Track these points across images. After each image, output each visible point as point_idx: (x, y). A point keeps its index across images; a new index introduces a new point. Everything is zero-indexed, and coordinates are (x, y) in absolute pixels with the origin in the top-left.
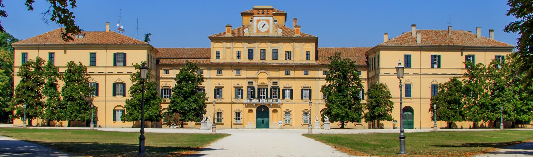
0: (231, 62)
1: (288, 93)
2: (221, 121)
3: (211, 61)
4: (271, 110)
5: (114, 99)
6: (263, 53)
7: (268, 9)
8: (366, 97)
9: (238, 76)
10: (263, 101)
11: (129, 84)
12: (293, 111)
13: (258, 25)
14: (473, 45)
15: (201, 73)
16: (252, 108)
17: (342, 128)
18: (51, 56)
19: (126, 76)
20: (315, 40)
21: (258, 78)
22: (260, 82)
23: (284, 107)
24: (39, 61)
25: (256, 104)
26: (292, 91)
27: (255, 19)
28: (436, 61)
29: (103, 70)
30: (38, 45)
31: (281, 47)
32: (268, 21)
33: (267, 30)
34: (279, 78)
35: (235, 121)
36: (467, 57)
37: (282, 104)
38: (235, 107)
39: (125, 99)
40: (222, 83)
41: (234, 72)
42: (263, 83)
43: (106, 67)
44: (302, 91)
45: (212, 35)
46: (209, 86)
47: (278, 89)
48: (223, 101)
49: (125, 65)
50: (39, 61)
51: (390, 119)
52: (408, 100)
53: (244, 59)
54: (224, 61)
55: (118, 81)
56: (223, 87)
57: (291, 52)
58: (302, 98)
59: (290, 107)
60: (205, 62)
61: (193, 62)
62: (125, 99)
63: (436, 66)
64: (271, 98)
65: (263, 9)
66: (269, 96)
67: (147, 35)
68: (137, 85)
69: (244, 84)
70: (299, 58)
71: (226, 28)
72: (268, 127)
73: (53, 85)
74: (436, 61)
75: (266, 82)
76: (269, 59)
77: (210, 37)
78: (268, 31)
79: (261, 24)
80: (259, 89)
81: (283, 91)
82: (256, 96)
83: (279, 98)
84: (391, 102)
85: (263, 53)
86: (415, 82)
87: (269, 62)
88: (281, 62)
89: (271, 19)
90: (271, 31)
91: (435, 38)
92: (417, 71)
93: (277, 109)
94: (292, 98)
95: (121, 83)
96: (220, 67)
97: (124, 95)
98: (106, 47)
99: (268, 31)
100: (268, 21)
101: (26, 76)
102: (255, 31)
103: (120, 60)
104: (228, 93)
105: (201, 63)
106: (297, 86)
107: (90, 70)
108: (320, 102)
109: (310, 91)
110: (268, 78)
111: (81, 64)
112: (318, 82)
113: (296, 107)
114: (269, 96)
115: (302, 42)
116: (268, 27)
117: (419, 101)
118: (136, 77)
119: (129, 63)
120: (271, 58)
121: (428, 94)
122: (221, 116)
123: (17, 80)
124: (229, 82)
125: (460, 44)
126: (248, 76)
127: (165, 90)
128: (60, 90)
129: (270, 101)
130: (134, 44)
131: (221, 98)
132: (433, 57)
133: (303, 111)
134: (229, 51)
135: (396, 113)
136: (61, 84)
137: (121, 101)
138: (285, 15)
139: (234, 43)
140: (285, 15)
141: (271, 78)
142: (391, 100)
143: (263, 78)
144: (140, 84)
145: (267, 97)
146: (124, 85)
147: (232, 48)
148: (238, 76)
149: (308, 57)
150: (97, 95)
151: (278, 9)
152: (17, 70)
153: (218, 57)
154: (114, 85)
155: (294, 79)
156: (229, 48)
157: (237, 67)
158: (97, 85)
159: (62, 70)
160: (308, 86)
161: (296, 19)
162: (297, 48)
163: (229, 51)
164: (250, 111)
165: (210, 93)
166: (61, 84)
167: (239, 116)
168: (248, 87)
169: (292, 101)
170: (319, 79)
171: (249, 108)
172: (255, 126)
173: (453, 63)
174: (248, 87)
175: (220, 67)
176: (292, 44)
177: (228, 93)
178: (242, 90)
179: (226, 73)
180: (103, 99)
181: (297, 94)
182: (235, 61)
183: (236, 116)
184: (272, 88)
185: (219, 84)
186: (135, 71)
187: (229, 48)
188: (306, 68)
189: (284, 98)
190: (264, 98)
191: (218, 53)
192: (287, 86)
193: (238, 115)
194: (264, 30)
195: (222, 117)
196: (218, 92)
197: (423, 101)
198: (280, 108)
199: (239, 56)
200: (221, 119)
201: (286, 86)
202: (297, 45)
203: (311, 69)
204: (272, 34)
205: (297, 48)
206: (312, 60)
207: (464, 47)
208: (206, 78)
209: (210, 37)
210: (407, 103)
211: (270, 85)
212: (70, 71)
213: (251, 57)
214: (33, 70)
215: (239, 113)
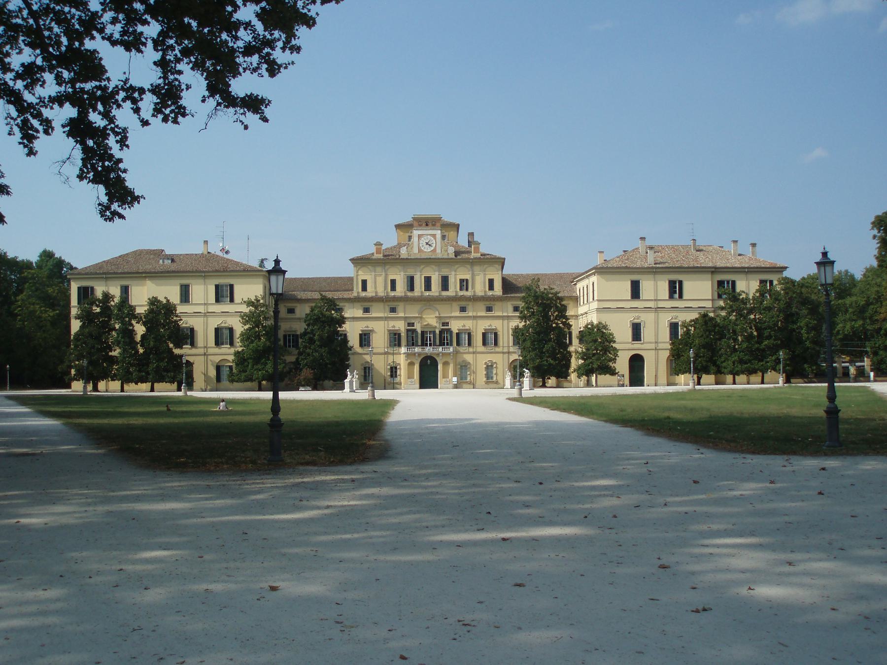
3: (355, 294)
5: (217, 350)
6: (428, 280)
8: (575, 341)
9: (393, 315)
10: (428, 350)
11: (239, 328)
14: (728, 265)
15: (340, 310)
16: (414, 361)
17: (544, 386)
18: (125, 290)
19: (233, 316)
20: (502, 262)
21: (421, 318)
24: (107, 297)
25: (419, 354)
26: (469, 335)
27: (416, 233)
28: (675, 290)
29: (201, 309)
30: (105, 273)
32: (434, 236)
36: (720, 283)
38: (391, 357)
39: (232, 350)
40: (371, 325)
41: (388, 309)
43: (205, 304)
44: (484, 335)
46: (352, 330)
47: (449, 331)
48: (375, 351)
49: (232, 300)
50: (107, 297)
51: (613, 372)
52: (637, 345)
55: (223, 325)
56: (372, 331)
57: (467, 280)
60: (346, 295)
61: (329, 295)
62: (232, 350)
63: (677, 296)
64: (442, 344)
66: (438, 342)
67: (262, 261)
68: (250, 329)
69: (401, 326)
70: (479, 287)
72: (436, 386)
73: (128, 333)
74: (675, 290)
77: (353, 260)
78: (434, 250)
79: (423, 241)
80: (423, 332)
82: (420, 343)
83: (451, 345)
84: (615, 349)
85: (428, 280)
86: (648, 320)
87: (437, 294)
89: (438, 233)
90: (438, 250)
91: (673, 255)
92: (651, 304)
94: (469, 344)
95: (226, 328)
96: (367, 304)
97: (232, 344)
98: (202, 274)
100: (434, 236)
101: (87, 317)
102: (416, 250)
103: (224, 294)
104: (380, 341)
105: (341, 297)
107: (180, 309)
108: (511, 349)
109: (496, 334)
111: (168, 301)
112: (507, 322)
113: (478, 358)
117: (653, 346)
118: (246, 318)
119: (237, 298)
121: (665, 335)
123: (76, 326)
125: (710, 265)
127: (289, 335)
128: (138, 338)
129: (440, 349)
130: (244, 271)
131: (369, 345)
132: (672, 284)
134: (380, 280)
135: (622, 365)
136: (140, 330)
137: (227, 354)
138: (456, 227)
140: (456, 227)
142: (614, 345)
144: (253, 328)
146: (231, 330)
147: (386, 275)
149: (491, 287)
150: (193, 344)
151: (447, 218)
152: (74, 311)
153: (364, 288)
154: (217, 330)
155: (475, 318)
158: (192, 330)
159: (141, 310)
161: (471, 235)
165: (354, 341)
166: (140, 330)
167: (396, 372)
168: (408, 330)
169: (471, 350)
172: (418, 385)
173: (700, 293)
174: (408, 330)
175: (367, 304)
178: (399, 335)
180: (201, 351)
181: (478, 339)
184: (441, 332)
186: (245, 309)
188: (489, 303)
189: (458, 344)
190: (430, 345)
191: (364, 282)
193: (394, 371)
196: (365, 339)
197: (661, 346)
202: (477, 268)
204: (439, 254)
206: (498, 290)
207: (716, 268)
209: (353, 260)
210: (637, 348)
212: (151, 311)
213: (411, 286)
214: (98, 310)
215: (396, 368)
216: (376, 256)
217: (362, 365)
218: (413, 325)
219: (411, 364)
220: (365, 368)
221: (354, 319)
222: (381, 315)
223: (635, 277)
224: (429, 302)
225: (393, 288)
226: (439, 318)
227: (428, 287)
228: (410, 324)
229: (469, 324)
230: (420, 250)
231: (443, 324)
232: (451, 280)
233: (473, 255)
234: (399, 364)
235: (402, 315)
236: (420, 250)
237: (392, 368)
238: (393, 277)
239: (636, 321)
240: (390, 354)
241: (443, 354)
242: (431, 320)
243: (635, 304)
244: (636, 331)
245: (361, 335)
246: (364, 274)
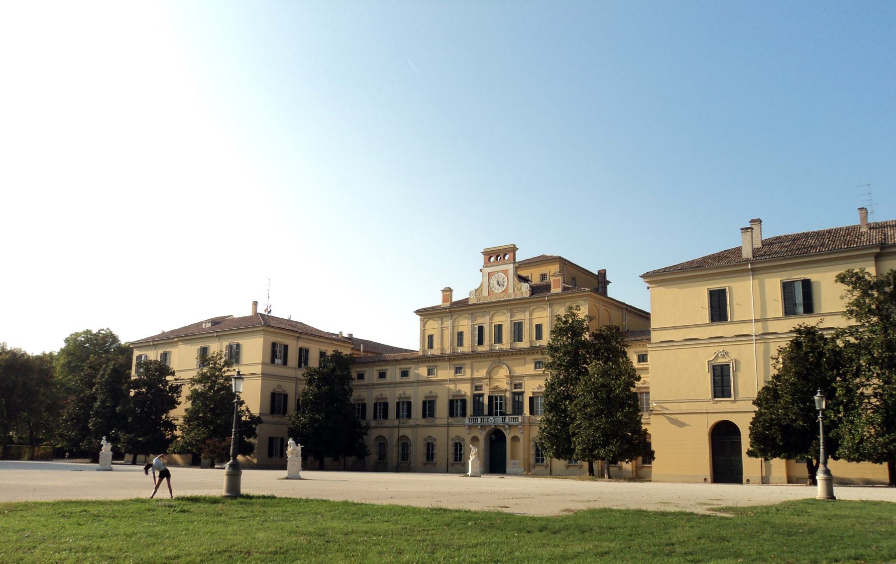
35: (451, 460)
42: (497, 387)
48: (438, 422)
52: (724, 404)
56: (436, 397)
63: (801, 309)
77: (418, 312)
78: (506, 291)
81: (531, 399)
100: (506, 272)
116: (506, 284)
122: (433, 450)
126: (476, 375)
157: (456, 360)
168: (475, 396)
174: (475, 396)
177: (442, 409)
178: (464, 402)
183: (456, 450)
189: (532, 412)
194: (498, 290)
200: (433, 454)
201: (536, 390)
209: (418, 312)
217: (425, 439)
220: (429, 444)
223: (717, 285)
224: (497, 357)
225: (460, 343)
226: (511, 377)
227: (499, 339)
228: (477, 388)
232: (526, 328)
234: (463, 440)
235: (468, 375)
239: (721, 361)
240: (453, 425)
241: (510, 426)
242: (501, 380)
243: (720, 329)
244: (722, 381)
245: (424, 403)
246: (433, 326)
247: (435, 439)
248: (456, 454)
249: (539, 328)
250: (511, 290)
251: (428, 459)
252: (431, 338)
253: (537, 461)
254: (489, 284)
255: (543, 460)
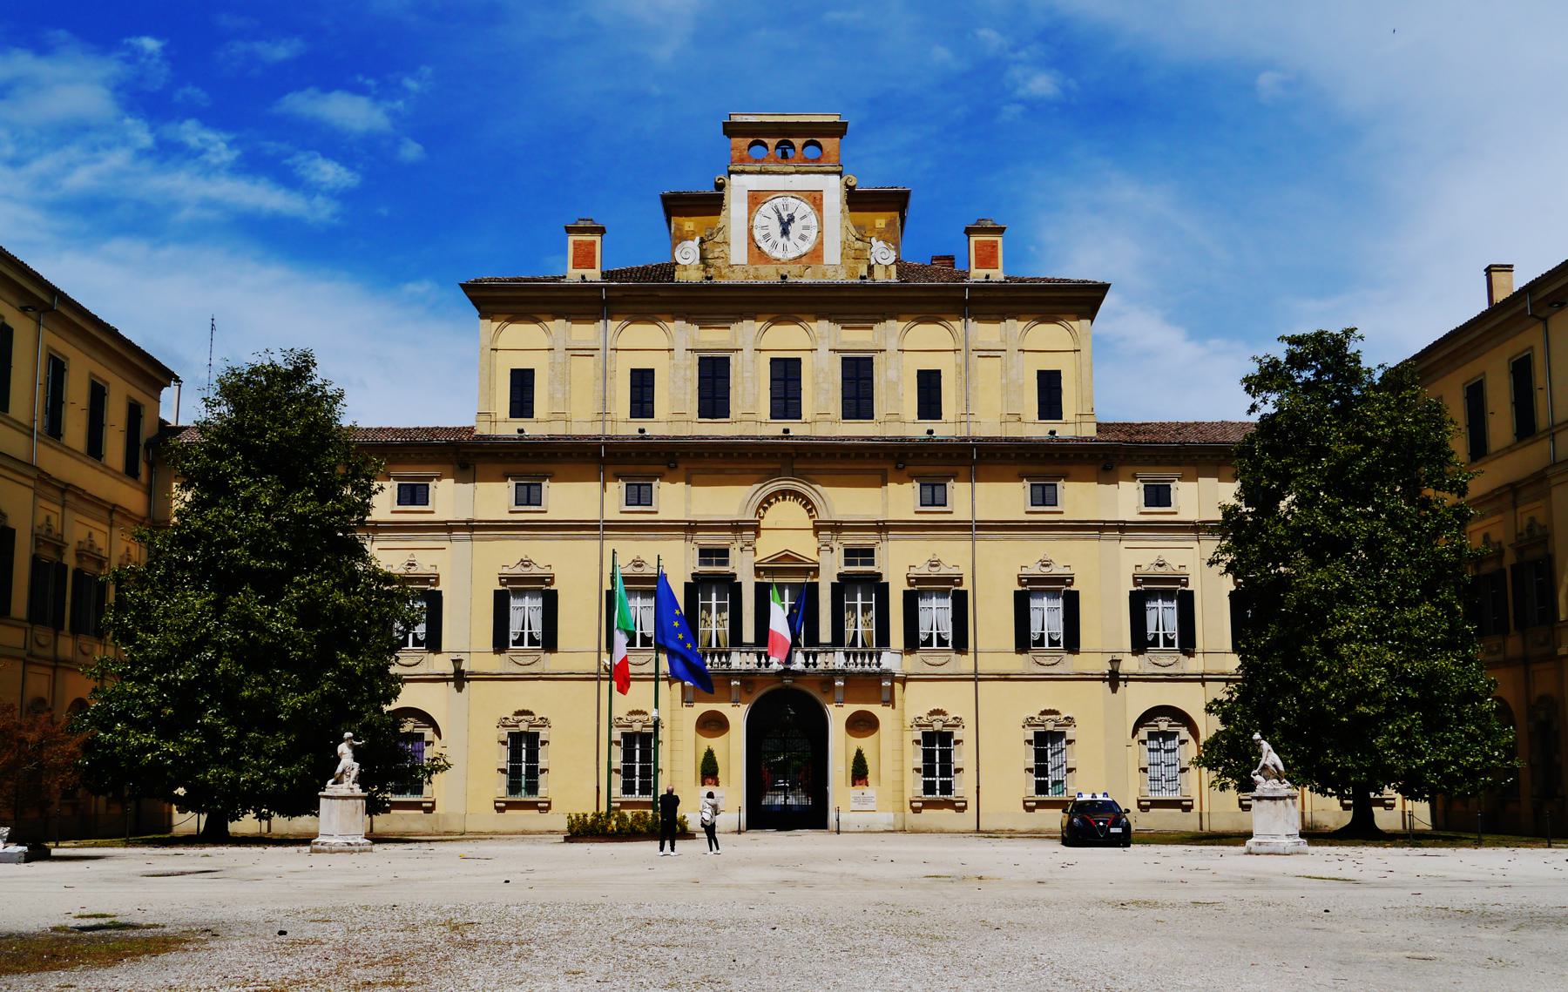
0: (595, 430)
1: (936, 614)
2: (533, 788)
4: (838, 715)
7: (813, 132)
12: (969, 721)
13: (758, 217)
16: (724, 708)
22: (768, 546)
23: (917, 701)
25: (747, 677)
31: (892, 344)
32: (815, 199)
33: (806, 247)
34: (882, 528)
37: (904, 680)
40: (544, 555)
41: (617, 489)
42: (787, 556)
45: (487, 272)
53: (676, 413)
54: (558, 429)
58: (1024, 641)
59: (954, 700)
65: (785, 132)
66: (825, 635)
71: (572, 239)
75: (805, 546)
76: (820, 414)
78: (816, 254)
81: (911, 601)
82: (749, 635)
83: (883, 639)
88: (893, 431)
90: (832, 255)
93: (876, 709)
99: (816, 254)
100: (815, 199)
106: (993, 573)
109: (1072, 605)
110: (818, 529)
114: (825, 635)
115: (1016, 316)
116: (812, 235)
120: (836, 408)
122: (533, 756)
124: (587, 550)
133: (1029, 722)
139: (613, 325)
141: (837, 527)
143: (787, 530)
145: (813, 639)
148: (638, 515)
156: (588, 352)
157: (637, 462)
160: (1057, 570)
162: (989, 353)
163: (585, 369)
164: (713, 724)
170: (1122, 528)
171: (702, 708)
176: (958, 325)
179: (567, 498)
182: (625, 427)
184: (842, 587)
185: (526, 563)
187: (588, 352)
189: (913, 642)
192: (934, 572)
194: (794, 247)
195: (542, 763)
198: (890, 702)
199: (642, 402)
200: (533, 772)
203: (1073, 469)
204: (834, 268)
205: (989, 353)
208: (448, 528)
211: (832, 566)
216: (573, 275)
218: (722, 554)
219: (713, 724)
221: (471, 527)
222: (591, 514)
228: (706, 554)
229: (952, 555)
230: (757, 253)
231: (851, 554)
233: (977, 275)
236: (757, 253)
237: (629, 739)
238: (642, 362)
246: (525, 342)
247: (545, 722)
248: (628, 772)
249: (929, 385)
250: (832, 255)
251: (514, 788)
252: (522, 382)
253: (929, 788)
254: (750, 230)
255: (947, 788)
